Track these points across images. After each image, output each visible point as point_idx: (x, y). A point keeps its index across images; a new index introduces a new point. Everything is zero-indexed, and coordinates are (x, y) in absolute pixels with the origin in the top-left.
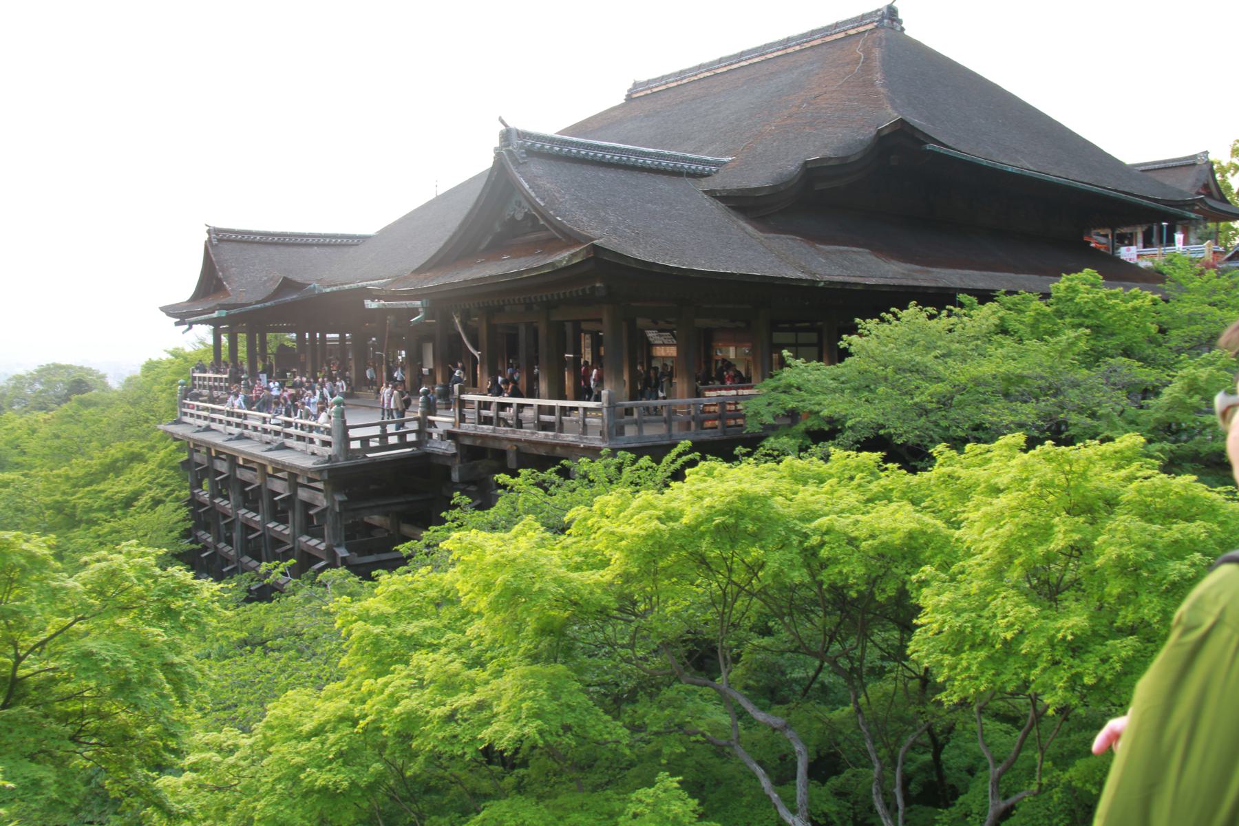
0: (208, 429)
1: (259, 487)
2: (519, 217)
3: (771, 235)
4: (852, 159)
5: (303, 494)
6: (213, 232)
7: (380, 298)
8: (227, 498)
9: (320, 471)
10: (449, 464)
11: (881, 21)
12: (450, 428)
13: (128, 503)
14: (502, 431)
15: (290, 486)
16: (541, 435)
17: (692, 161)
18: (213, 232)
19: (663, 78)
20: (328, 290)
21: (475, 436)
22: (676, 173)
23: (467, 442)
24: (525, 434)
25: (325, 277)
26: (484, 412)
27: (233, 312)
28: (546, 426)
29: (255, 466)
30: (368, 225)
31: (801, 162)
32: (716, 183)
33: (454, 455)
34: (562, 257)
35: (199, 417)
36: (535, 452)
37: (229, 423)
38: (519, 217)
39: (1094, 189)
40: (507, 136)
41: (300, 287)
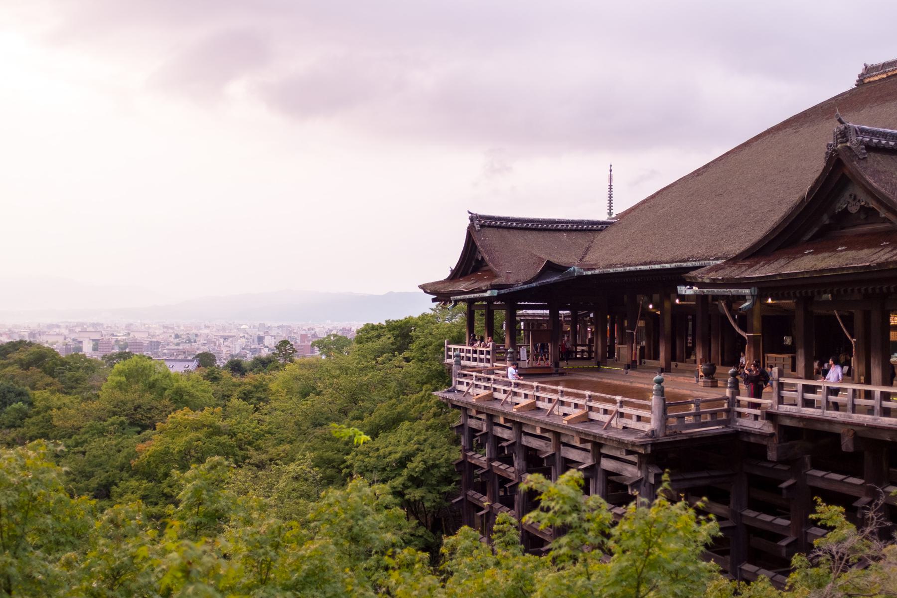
1: (553, 455)
5: (607, 464)
7: (691, 285)
9: (644, 446)
10: (765, 443)
15: (594, 456)
20: (589, 273)
21: (802, 418)
23: (788, 422)
27: (503, 291)
29: (547, 435)
33: (772, 435)
38: (853, 210)
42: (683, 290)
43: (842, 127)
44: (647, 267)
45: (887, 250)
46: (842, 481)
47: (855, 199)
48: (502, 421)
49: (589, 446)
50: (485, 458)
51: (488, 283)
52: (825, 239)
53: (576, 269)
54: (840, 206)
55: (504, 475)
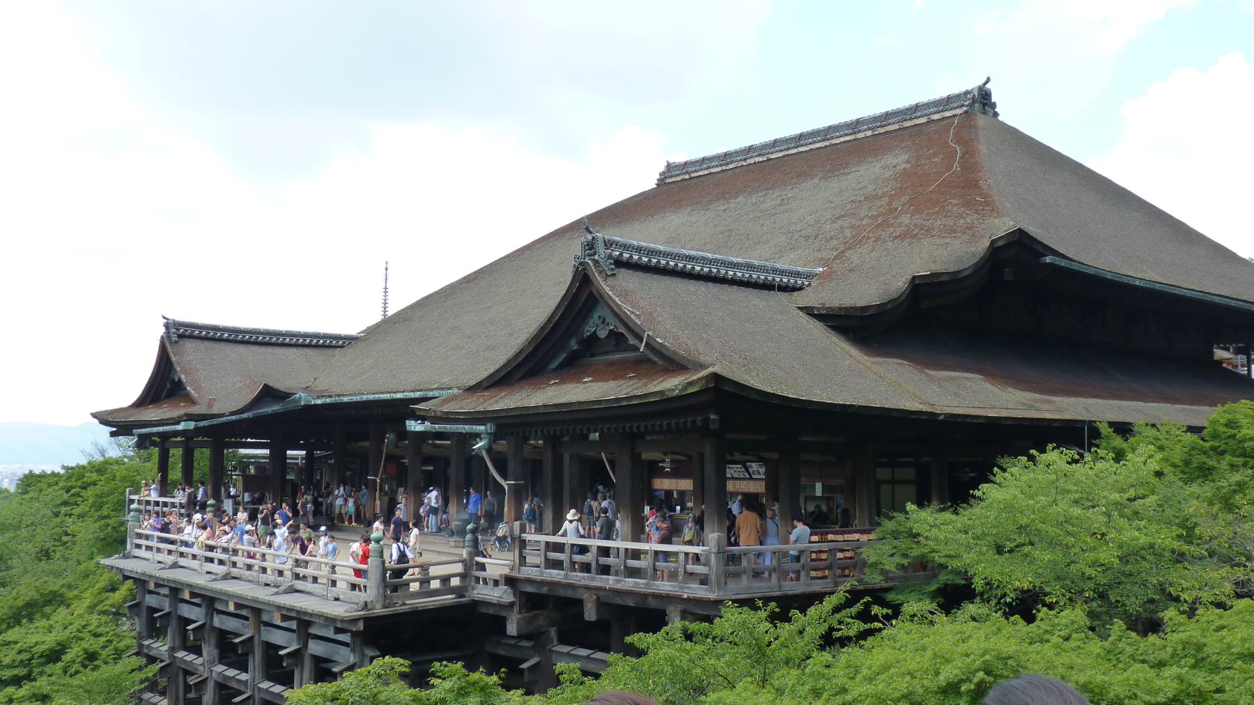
0: (175, 566)
1: (251, 638)
2: (602, 334)
3: (878, 359)
4: (964, 274)
5: (315, 648)
6: (170, 326)
7: (423, 419)
8: (197, 651)
9: (354, 621)
10: (504, 614)
11: (971, 105)
12: (506, 571)
13: (54, 656)
14: (579, 578)
15: (299, 638)
16: (629, 583)
17: (782, 272)
18: (170, 326)
19: (704, 159)
20: (319, 402)
21: (543, 583)
22: (767, 287)
23: (530, 589)
24: (610, 582)
25: (314, 383)
26: (553, 555)
27: (202, 424)
28: (634, 573)
29: (244, 612)
31: (910, 277)
32: (808, 298)
33: (512, 605)
34: (671, 384)
35: (159, 550)
36: (621, 602)
38: (602, 334)
39: (1233, 303)
41: (281, 396)
42: (414, 426)
43: (590, 237)
44: (386, 396)
45: (631, 382)
46: (588, 657)
47: (603, 322)
48: (187, 596)
49: (293, 625)
50: (166, 648)
51: (182, 412)
52: (573, 367)
53: (304, 398)
54: (589, 329)
55: (189, 668)
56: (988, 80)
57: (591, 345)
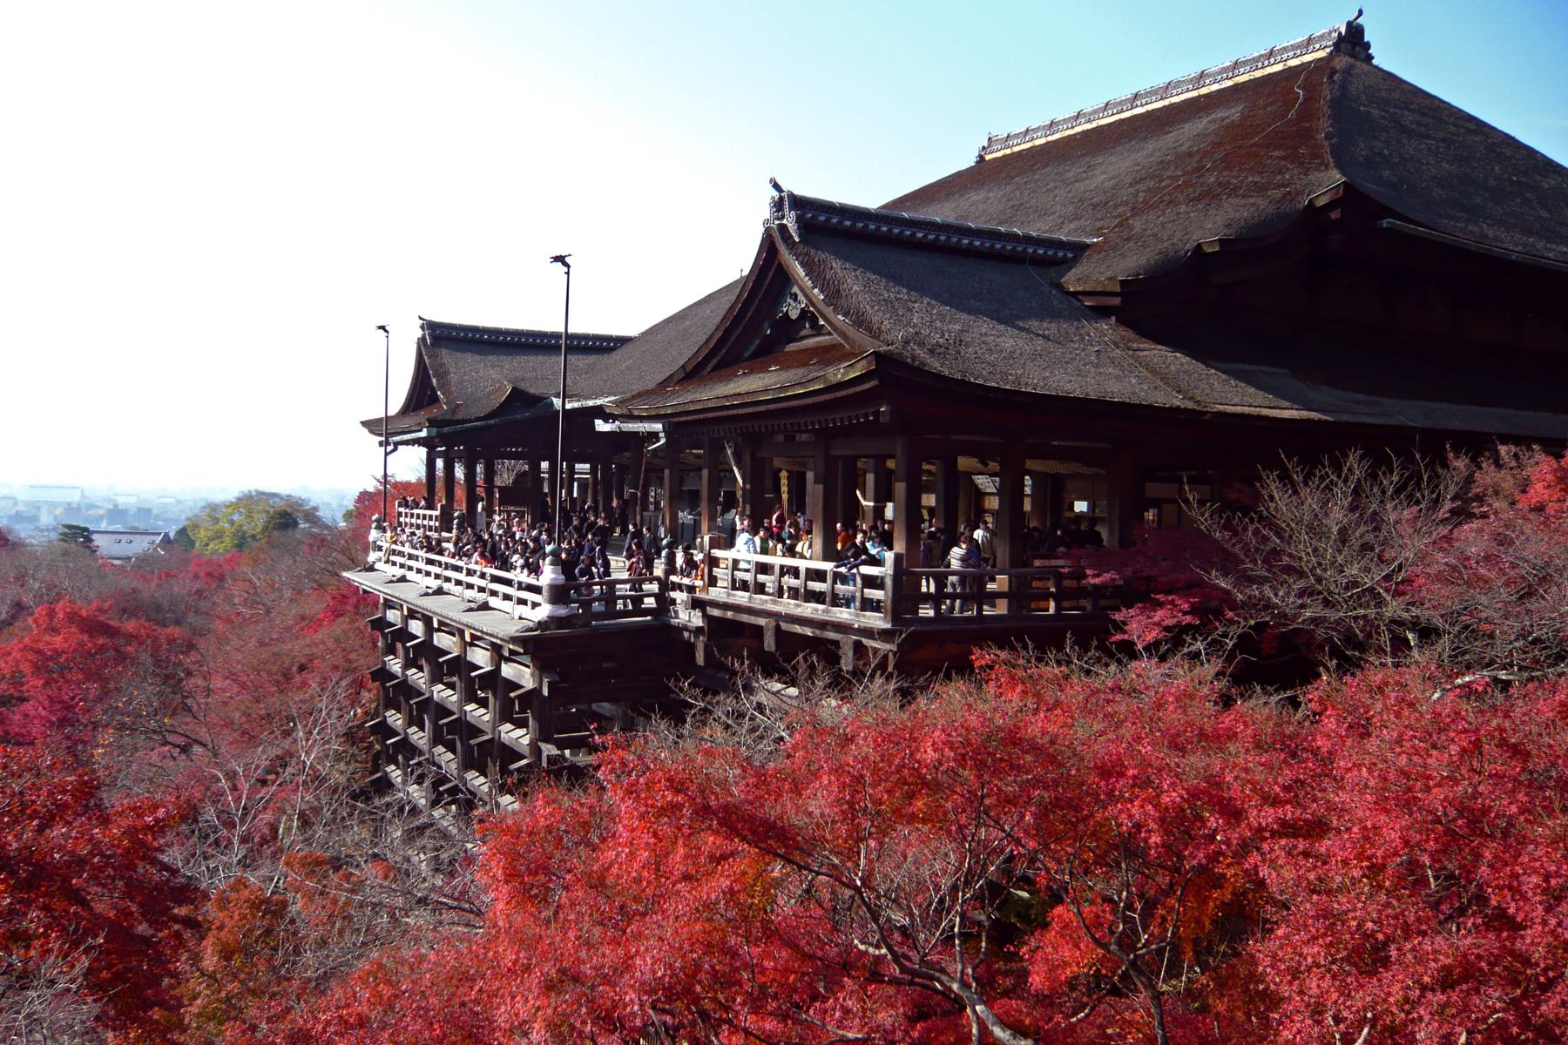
1: (458, 657)
2: (794, 315)
16: (809, 609)
21: (725, 606)
23: (716, 612)
24: (788, 606)
28: (818, 597)
30: (630, 327)
33: (699, 630)
37: (428, 574)
38: (794, 315)
40: (778, 205)
42: (601, 426)
56: (1361, 13)
57: (789, 330)
